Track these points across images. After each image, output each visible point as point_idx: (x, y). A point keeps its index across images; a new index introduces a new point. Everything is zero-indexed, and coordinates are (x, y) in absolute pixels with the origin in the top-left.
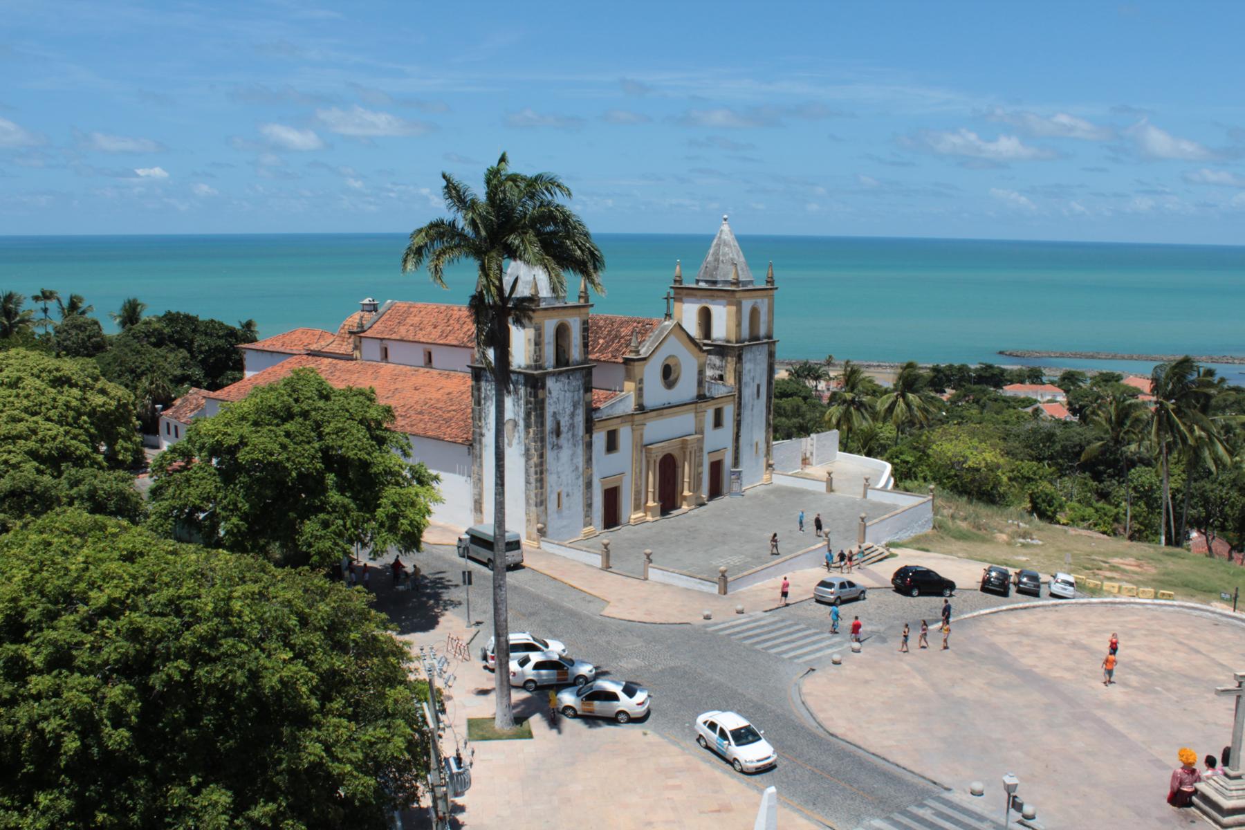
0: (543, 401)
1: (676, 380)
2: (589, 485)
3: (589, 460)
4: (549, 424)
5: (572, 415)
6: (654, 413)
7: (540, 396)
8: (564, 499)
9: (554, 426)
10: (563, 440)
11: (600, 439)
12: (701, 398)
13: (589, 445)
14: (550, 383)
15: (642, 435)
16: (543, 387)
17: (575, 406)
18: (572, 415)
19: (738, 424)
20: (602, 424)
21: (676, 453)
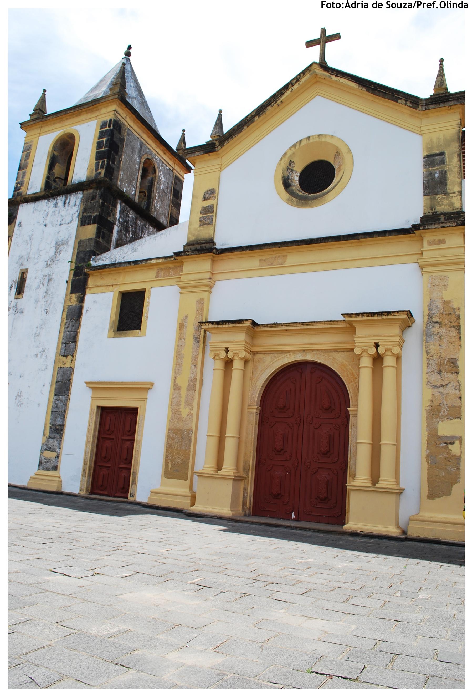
2: (63, 386)
6: (252, 261)
11: (101, 305)
13: (74, 316)
15: (201, 305)
20: (108, 279)
21: (336, 363)
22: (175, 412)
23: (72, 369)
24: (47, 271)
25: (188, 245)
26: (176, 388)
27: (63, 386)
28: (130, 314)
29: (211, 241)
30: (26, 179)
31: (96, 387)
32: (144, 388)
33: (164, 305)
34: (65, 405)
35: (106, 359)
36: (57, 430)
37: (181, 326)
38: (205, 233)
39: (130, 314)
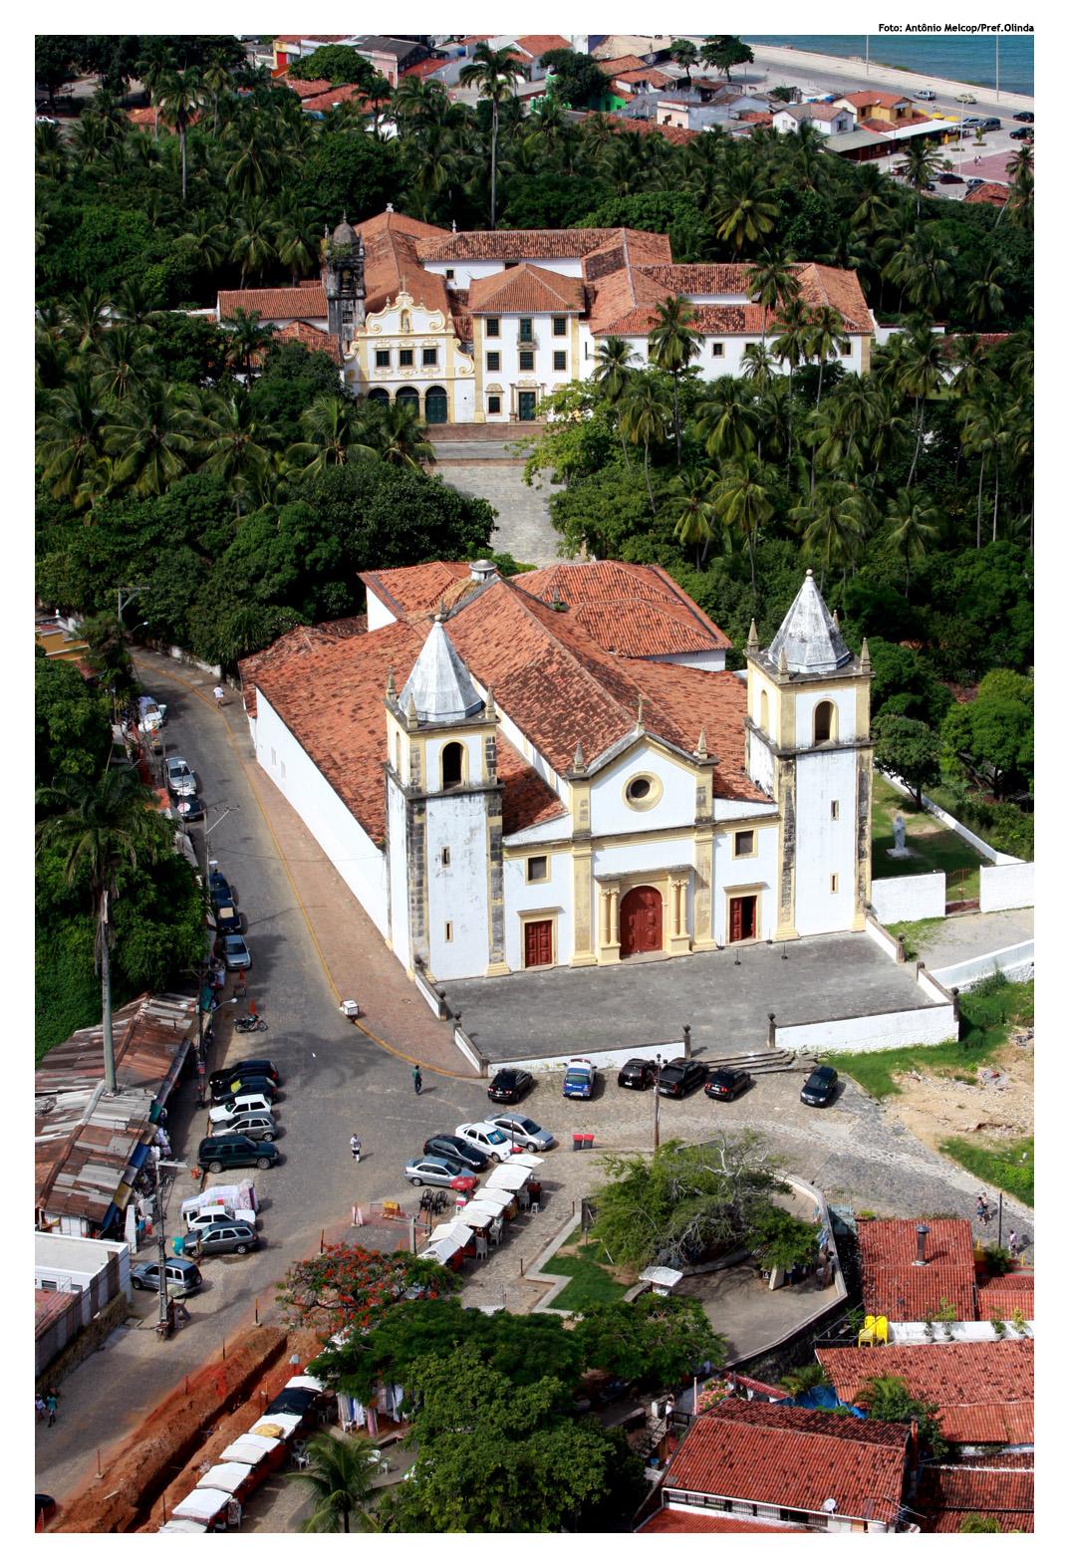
0: (421, 826)
1: (658, 799)
2: (498, 916)
3: (498, 890)
4: (432, 851)
5: (469, 841)
7: (417, 820)
8: (455, 931)
9: (441, 853)
10: (450, 869)
12: (706, 824)
13: (498, 874)
14: (430, 806)
16: (422, 811)
17: (472, 830)
18: (469, 841)
19: (790, 851)
22: (578, 920)
23: (502, 906)
24: (467, 847)
25: (575, 833)
26: (577, 908)
27: (498, 916)
28: (536, 869)
29: (589, 831)
30: (422, 775)
31: (523, 914)
32: (556, 911)
33: (562, 866)
34: (502, 927)
35: (522, 896)
36: (499, 940)
37: (577, 877)
38: (584, 825)
39: (536, 869)
